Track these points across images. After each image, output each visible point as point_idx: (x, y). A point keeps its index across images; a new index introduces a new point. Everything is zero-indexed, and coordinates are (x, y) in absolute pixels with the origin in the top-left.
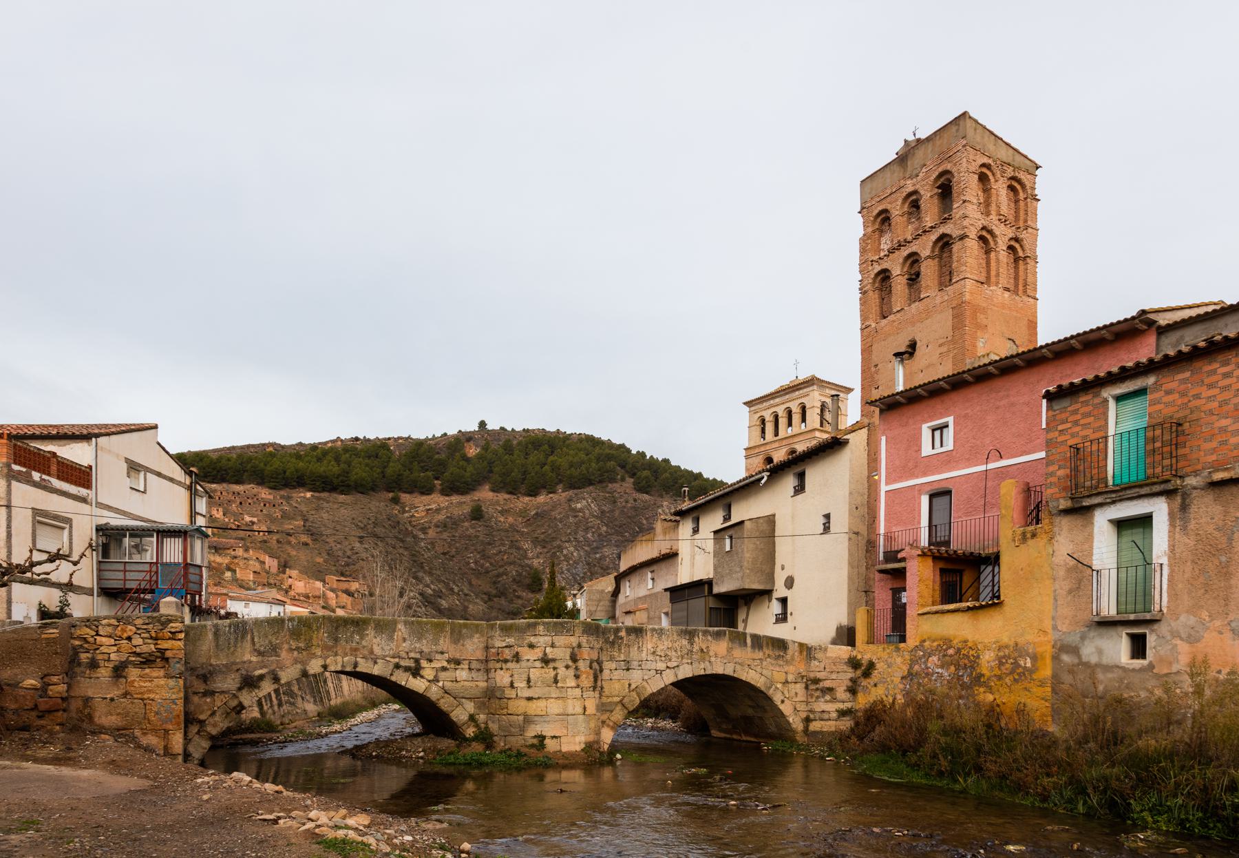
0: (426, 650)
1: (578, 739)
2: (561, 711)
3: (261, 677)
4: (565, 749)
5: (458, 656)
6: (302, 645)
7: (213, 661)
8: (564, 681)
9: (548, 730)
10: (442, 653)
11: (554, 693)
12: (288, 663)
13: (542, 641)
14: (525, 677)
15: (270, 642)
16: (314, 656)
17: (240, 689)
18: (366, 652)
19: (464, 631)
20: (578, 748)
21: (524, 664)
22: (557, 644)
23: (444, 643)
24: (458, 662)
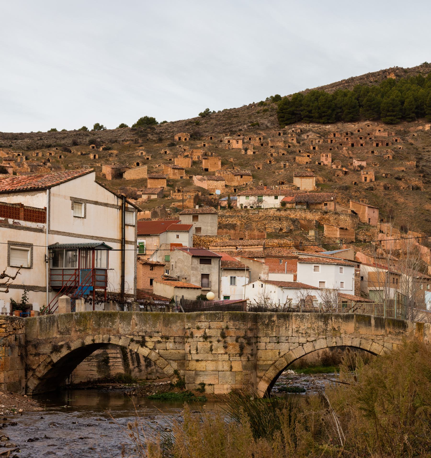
0: (149, 331)
1: (226, 386)
2: (214, 368)
3: (62, 346)
4: (217, 392)
5: (167, 334)
6: (81, 328)
7: (39, 338)
8: (217, 349)
9: (207, 380)
10: (158, 332)
11: (210, 357)
12: (75, 338)
13: (203, 325)
14: (195, 347)
15: (66, 327)
16: (88, 334)
17: (52, 353)
18: (115, 332)
19: (171, 319)
20: (226, 392)
21: (195, 339)
22: (212, 327)
23: (159, 326)
24: (167, 338)
